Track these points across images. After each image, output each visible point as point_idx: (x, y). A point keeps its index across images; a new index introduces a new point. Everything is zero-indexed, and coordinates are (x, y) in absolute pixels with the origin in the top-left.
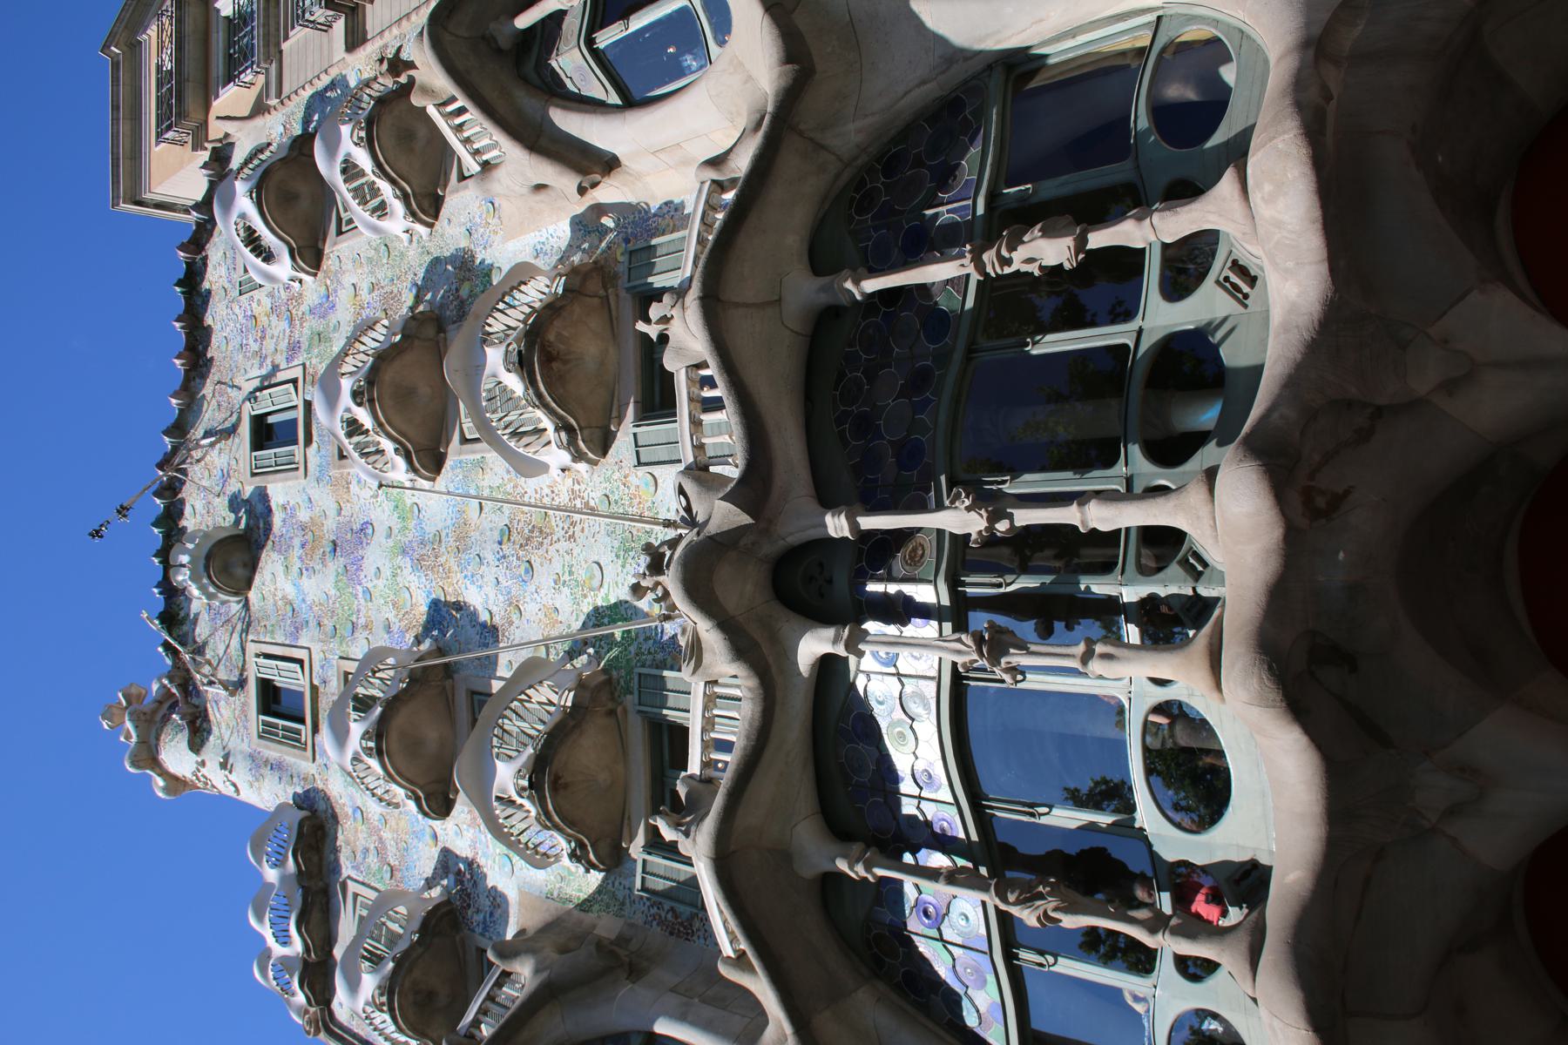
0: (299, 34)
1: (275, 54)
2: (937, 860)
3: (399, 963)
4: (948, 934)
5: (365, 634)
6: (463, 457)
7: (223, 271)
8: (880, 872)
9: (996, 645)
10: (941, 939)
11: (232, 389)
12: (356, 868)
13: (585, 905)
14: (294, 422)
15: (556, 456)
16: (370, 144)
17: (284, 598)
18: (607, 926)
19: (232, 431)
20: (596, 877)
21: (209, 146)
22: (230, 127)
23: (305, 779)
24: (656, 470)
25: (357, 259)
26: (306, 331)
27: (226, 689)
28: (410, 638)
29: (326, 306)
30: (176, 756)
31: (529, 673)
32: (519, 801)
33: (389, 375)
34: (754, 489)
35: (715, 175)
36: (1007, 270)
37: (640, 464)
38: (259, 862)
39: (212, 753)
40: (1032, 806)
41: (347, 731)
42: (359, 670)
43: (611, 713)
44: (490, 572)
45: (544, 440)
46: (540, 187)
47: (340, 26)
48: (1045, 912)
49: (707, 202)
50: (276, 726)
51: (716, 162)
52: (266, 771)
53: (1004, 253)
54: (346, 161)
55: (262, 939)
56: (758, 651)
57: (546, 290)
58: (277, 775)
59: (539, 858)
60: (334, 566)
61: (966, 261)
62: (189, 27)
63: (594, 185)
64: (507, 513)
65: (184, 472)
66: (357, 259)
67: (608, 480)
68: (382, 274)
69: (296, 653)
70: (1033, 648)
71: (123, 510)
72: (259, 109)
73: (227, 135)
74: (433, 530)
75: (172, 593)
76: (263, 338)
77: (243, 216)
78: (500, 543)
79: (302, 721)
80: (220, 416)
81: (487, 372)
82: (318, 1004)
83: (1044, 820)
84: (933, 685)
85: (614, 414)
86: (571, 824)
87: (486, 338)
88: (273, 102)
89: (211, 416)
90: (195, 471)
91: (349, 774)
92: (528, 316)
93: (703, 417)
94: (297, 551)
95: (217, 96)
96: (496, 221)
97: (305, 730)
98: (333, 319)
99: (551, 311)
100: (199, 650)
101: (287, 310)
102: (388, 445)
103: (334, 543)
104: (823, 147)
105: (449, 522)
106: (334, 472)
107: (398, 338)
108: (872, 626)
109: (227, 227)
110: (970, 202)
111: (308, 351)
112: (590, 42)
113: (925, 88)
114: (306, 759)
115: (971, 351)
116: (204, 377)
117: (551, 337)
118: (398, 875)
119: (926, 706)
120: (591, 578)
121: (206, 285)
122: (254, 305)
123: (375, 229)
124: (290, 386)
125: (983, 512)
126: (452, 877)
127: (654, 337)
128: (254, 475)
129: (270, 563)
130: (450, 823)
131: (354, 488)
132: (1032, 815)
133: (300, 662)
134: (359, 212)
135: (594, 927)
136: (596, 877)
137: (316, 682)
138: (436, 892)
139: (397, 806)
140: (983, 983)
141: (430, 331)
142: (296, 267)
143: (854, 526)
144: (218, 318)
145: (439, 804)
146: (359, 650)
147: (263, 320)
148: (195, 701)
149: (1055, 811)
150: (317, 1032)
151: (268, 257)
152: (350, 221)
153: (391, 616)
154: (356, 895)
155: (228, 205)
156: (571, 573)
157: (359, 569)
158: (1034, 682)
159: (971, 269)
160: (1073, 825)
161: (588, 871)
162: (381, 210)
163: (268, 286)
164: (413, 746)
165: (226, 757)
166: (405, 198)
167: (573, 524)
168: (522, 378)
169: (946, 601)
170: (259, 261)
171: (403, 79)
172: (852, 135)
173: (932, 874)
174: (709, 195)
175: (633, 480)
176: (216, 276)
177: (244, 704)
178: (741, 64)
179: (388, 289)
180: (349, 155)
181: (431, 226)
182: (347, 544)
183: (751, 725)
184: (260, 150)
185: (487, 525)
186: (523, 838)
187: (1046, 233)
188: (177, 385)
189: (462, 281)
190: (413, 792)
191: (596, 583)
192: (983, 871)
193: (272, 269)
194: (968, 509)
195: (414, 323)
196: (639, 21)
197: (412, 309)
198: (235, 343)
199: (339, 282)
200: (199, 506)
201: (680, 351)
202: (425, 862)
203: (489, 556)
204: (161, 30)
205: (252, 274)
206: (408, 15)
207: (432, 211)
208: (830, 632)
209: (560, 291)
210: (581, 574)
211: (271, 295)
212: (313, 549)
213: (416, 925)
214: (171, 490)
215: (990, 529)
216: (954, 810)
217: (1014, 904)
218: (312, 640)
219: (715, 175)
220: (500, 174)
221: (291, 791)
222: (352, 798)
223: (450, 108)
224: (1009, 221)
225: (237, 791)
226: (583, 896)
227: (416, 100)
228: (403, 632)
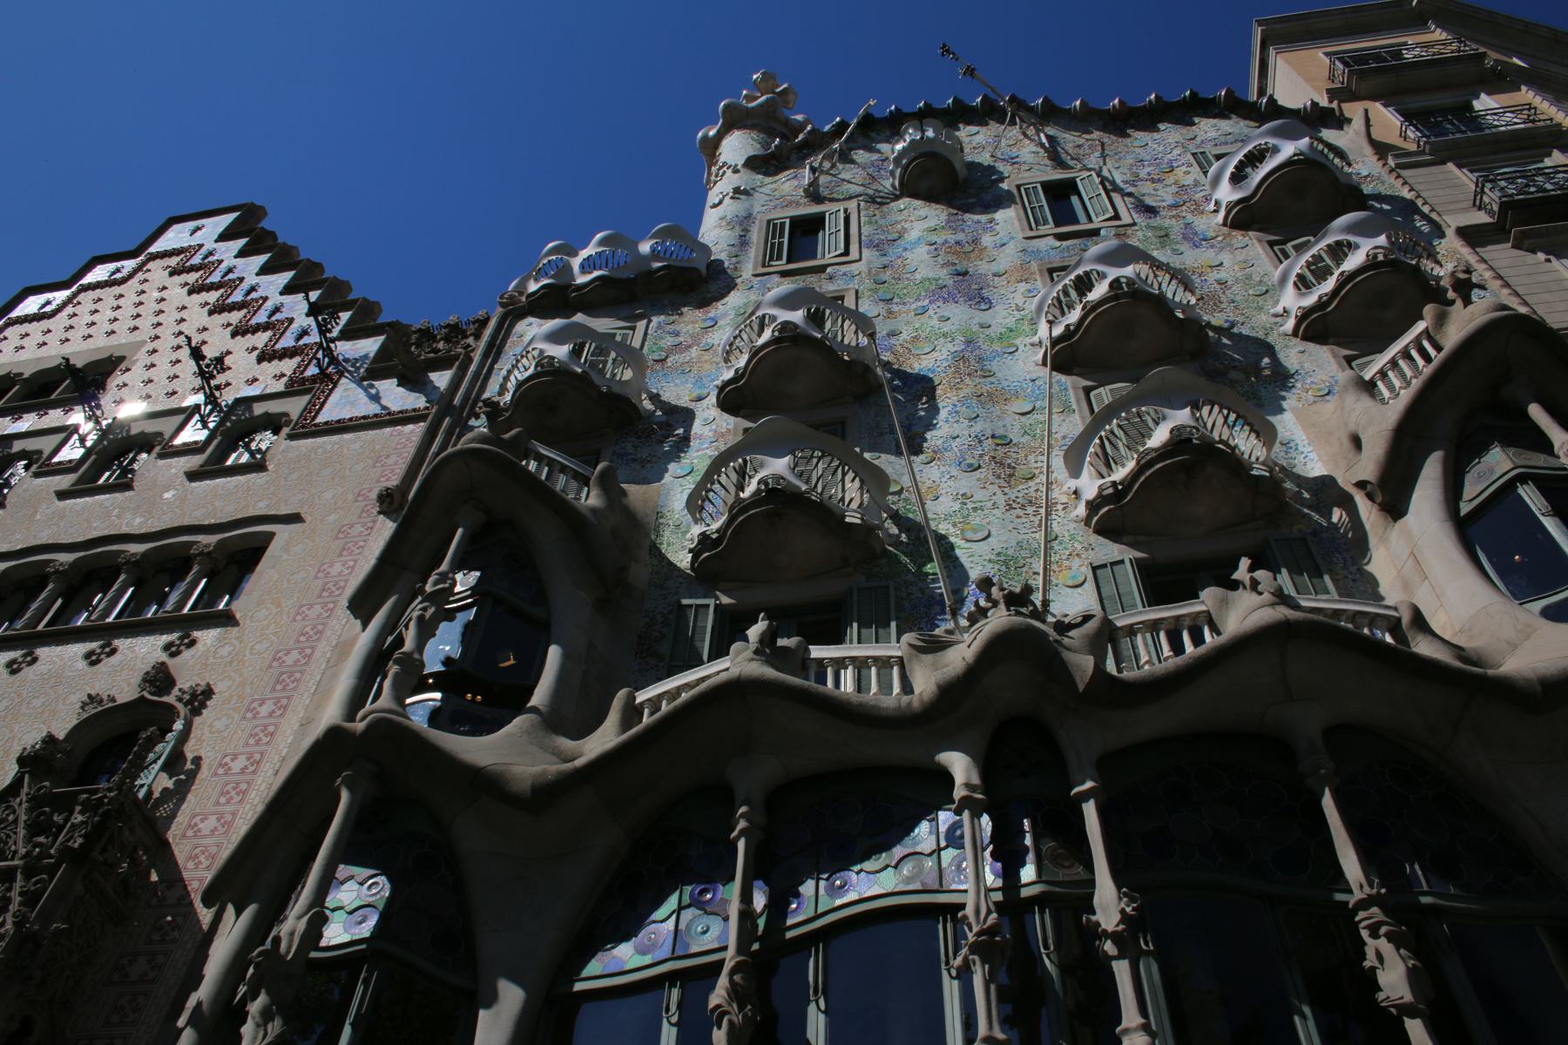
0: (1466, 180)
1: (1440, 156)
2: (759, 901)
3: (584, 377)
4: (687, 915)
5: (883, 313)
6: (1071, 392)
7: (1212, 134)
8: (741, 845)
9: (986, 948)
11: (1099, 160)
12: (659, 327)
13: (655, 551)
14: (1076, 221)
15: (1089, 485)
16: (1371, 264)
17: (905, 230)
18: (640, 573)
19: (1060, 163)
20: (683, 560)
21: (1335, 105)
22: (1358, 123)
23: (736, 269)
24: (1090, 586)
25: (1247, 264)
26: (1167, 223)
27: (810, 185)
28: (886, 356)
29: (1194, 238)
30: (736, 147)
31: (875, 480)
34: (1108, 691)
35: (1405, 620)
36: (1365, 934)
37: (1094, 569)
38: (652, 237)
39: (745, 179)
40: (825, 992)
41: (794, 308)
42: (848, 310)
44: (962, 428)
45: (1104, 471)
46: (1356, 442)
47: (1482, 218)
48: (726, 1013)
49: (1378, 615)
50: (781, 236)
51: (1419, 622)
52: (738, 231)
53: (1383, 930)
54: (1349, 245)
55: (585, 247)
56: (952, 709)
57: (1253, 459)
58: (736, 242)
59: (696, 505)
60: (944, 275)
61: (1367, 889)
63: (1370, 497)
64: (1023, 440)
65: (1013, 123)
66: (1247, 264)
67: (1072, 538)
68: (1237, 292)
69: (854, 248)
70: (993, 987)
71: (970, 71)
72: (1382, 150)
73: (1349, 121)
74: (995, 369)
75: (892, 125)
76: (1153, 181)
77: (1276, 150)
78: (993, 436)
79: (789, 261)
80: (1069, 147)
81: (1166, 411)
82: (530, 303)
83: (812, 1008)
84: (936, 887)
87: (1196, 407)
88: (1391, 162)
89: (1069, 140)
90: (1014, 132)
91: (753, 313)
92: (1225, 443)
93: (1162, 635)
94: (952, 238)
95: (1386, 106)
96: (1312, 399)
97: (781, 264)
99: (1233, 463)
100: (845, 157)
101: (1185, 200)
102: (1074, 316)
103: (966, 273)
105: (1005, 384)
106: (1034, 266)
107: (1180, 316)
108: (986, 821)
109: (1261, 135)
110: (1425, 888)
111: (1149, 227)
112: (1523, 478)
114: (755, 268)
116: (1104, 129)
118: (658, 366)
119: (909, 880)
120: (975, 531)
121: (1196, 120)
122: (1184, 169)
123: (1283, 280)
124: (1111, 213)
125: (1121, 927)
126: (664, 418)
127: (1235, 576)
128: (1018, 187)
130: (715, 412)
131: (1023, 287)
132: (816, 992)
133: (846, 253)
134: (1299, 264)
136: (683, 560)
137: (829, 270)
138: (647, 405)
139: (727, 360)
140: (642, 951)
142: (1231, 206)
143: (1085, 796)
144: (1164, 134)
145: (731, 400)
146: (867, 307)
147: (1171, 179)
148: (794, 156)
149: (822, 1017)
150: (503, 305)
151: (1238, 178)
152: (1287, 257)
153: (904, 336)
154: (633, 328)
155: (1287, 134)
156: (975, 509)
157: (945, 301)
158: (951, 990)
159: (1358, 895)
160: (811, 1035)
161: (691, 551)
162: (1303, 284)
165: (746, 193)
166: (1320, 305)
167: (1023, 507)
168: (1165, 445)
169: (1025, 892)
170: (1231, 169)
171: (1451, 294)
173: (746, 897)
174: (1385, 616)
175: (1076, 563)
176: (1208, 129)
177: (798, 204)
178: (1528, 637)
179: (1223, 298)
180: (1357, 247)
181: (1295, 333)
182: (968, 286)
183: (874, 707)
184: (1340, 153)
185: (1008, 421)
186: (716, 487)
187: (1412, 974)
188: (1096, 104)
190: (743, 375)
191: (969, 535)
192: (756, 946)
193: (1225, 183)
194: (1123, 911)
196: (1551, 525)
197: (1208, 324)
198: (1142, 154)
199: (1222, 249)
200: (980, 138)
201: (1224, 603)
202: (676, 392)
203: (978, 427)
204: (1444, 43)
205: (1216, 165)
206: (1507, 285)
208: (976, 780)
209: (1254, 472)
210: (976, 519)
211: (1196, 183)
212: (956, 253)
213: (616, 389)
214: (988, 113)
216: (811, 913)
217: (731, 981)
218: (869, 262)
219: (1405, 620)
220: (1366, 402)
221: (723, 256)
222: (725, 315)
223: (1426, 344)
224: (1413, 932)
225: (715, 206)
226: (664, 548)
227: (1429, 310)
228: (891, 349)
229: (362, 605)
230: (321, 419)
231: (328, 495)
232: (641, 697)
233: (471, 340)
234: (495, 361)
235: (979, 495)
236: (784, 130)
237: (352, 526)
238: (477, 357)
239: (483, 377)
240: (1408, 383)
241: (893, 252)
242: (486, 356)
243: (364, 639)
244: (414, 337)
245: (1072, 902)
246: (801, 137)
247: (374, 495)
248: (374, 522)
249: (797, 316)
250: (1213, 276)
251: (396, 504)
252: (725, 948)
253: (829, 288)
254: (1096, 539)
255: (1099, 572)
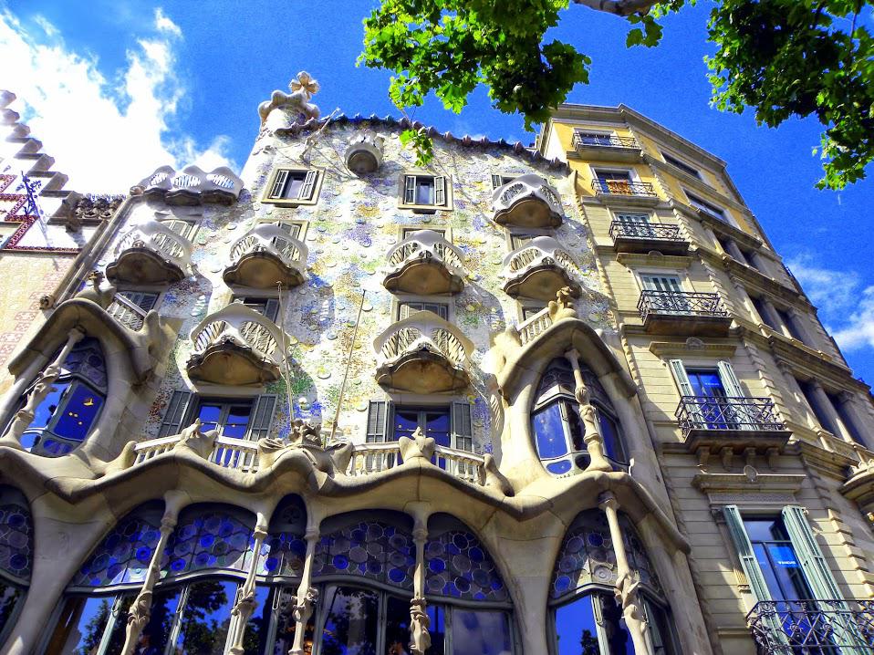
1: (601, 202)
3: (154, 254)
10: (131, 559)
26: (469, 213)
29: (479, 227)
32: (222, 335)
33: (433, 269)
36: (412, 616)
37: (371, 403)
43: (259, 380)
46: (505, 360)
52: (261, 174)
62: (625, 154)
72: (579, 190)
79: (283, 196)
85: (397, 391)
86: (209, 359)
94: (364, 200)
98: (472, 229)
99: (445, 364)
103: (363, 223)
104: (487, 522)
106: (397, 225)
107: (451, 273)
113: (507, 573)
115: (384, 591)
117: (433, 365)
118: (200, 248)
122: (487, 182)
124: (443, 203)
129: (361, 185)
133: (311, 199)
135: (162, 362)
137: (300, 207)
138: (189, 271)
141: (454, 288)
145: (231, 277)
153: (323, 254)
163: (494, 192)
164: (257, 269)
166: (518, 280)
172: (491, 536)
189: (475, 306)
193: (499, 201)
194: (305, 599)
195: (457, 281)
201: (406, 446)
206: (607, 282)
207: (511, 292)
210: (327, 366)
213: (174, 262)
215: (297, 609)
229: (17, 367)
230: (21, 244)
231: (15, 292)
232: (140, 446)
233: (110, 211)
234: (119, 228)
235: (333, 353)
236: (303, 112)
237: (24, 313)
238: (111, 222)
239: (111, 237)
240: (533, 337)
241: (334, 202)
242: (115, 223)
243: (13, 387)
244: (82, 202)
245: (292, 588)
246: (307, 123)
247: (40, 297)
248: (37, 313)
249: (265, 243)
250: (480, 248)
251: (50, 306)
252: (143, 583)
253: (297, 218)
254: (379, 388)
255: (373, 406)
